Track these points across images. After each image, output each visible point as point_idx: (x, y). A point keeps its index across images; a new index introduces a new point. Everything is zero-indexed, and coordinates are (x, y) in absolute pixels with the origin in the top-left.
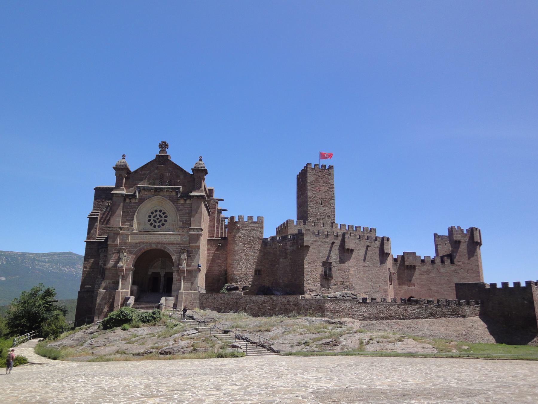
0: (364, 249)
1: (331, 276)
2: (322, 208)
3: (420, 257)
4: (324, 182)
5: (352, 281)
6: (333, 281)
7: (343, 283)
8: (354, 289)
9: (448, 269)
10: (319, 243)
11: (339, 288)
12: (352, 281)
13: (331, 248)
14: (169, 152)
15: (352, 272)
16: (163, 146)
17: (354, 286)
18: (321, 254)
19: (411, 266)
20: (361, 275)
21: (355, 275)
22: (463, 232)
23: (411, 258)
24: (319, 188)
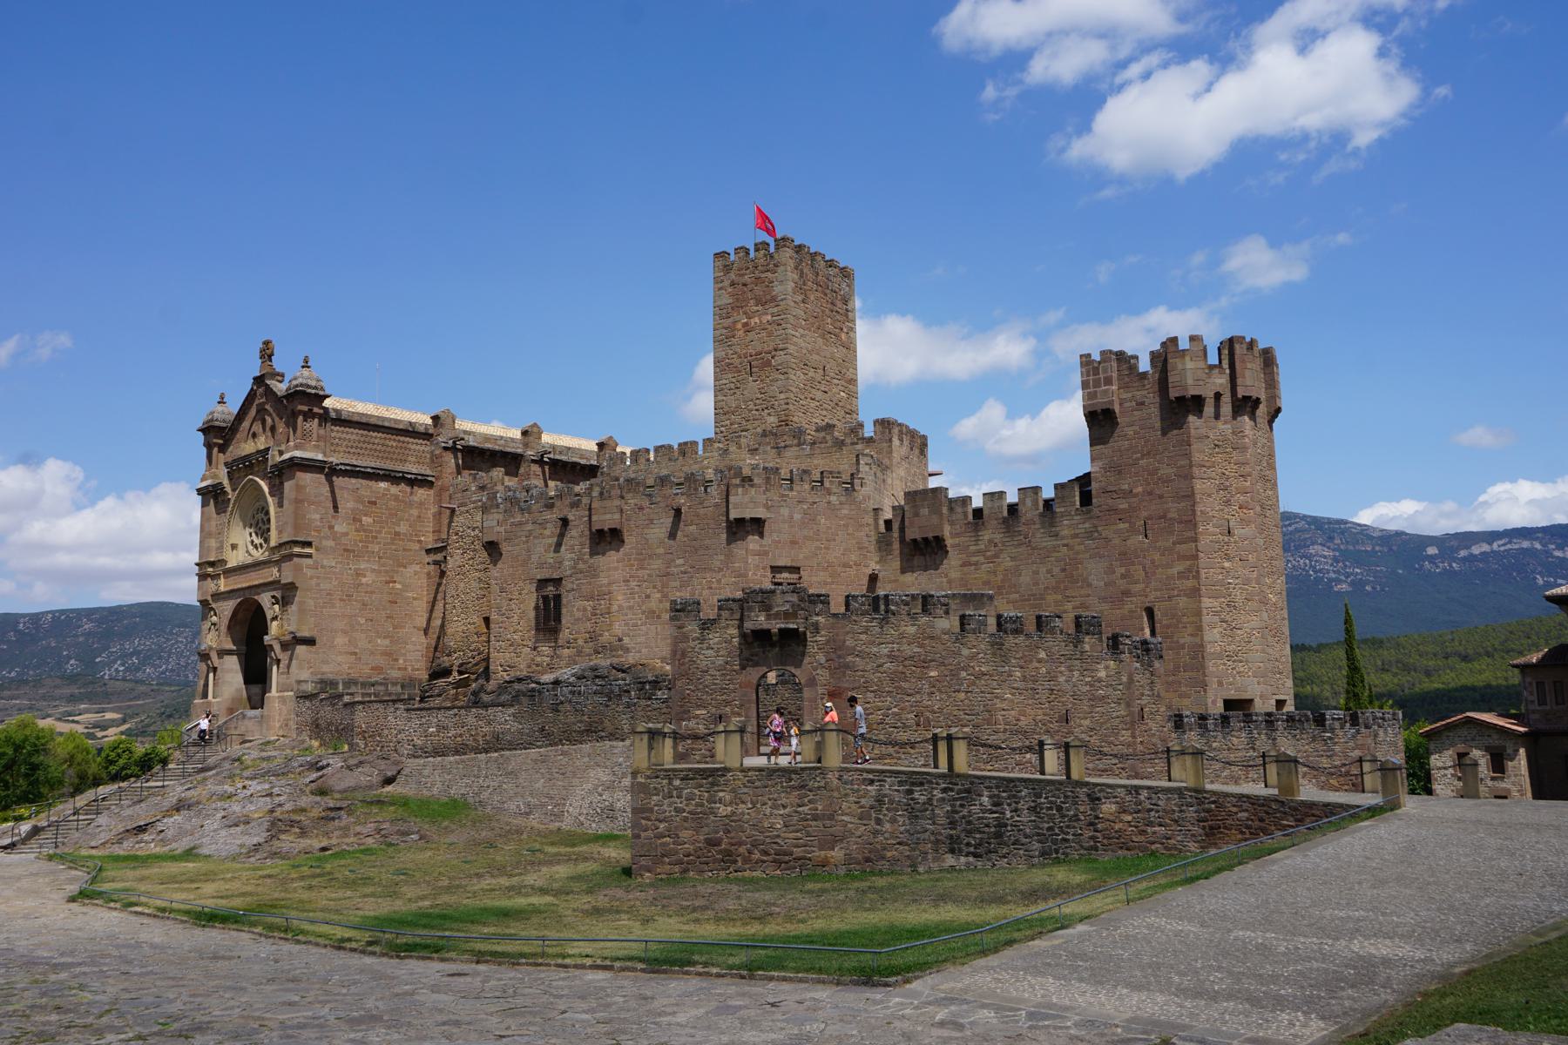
0: (668, 521)
1: (558, 619)
2: (752, 386)
3: (966, 500)
4: (759, 302)
5: (618, 628)
6: (565, 634)
7: (593, 637)
8: (627, 650)
9: (1065, 532)
10: (530, 527)
11: (579, 653)
12: (618, 628)
13: (562, 535)
14: (278, 364)
15: (620, 599)
16: (267, 353)
17: (626, 640)
18: (535, 558)
19: (925, 540)
20: (653, 604)
21: (631, 608)
22: (1133, 368)
23: (925, 511)
24: (745, 325)
